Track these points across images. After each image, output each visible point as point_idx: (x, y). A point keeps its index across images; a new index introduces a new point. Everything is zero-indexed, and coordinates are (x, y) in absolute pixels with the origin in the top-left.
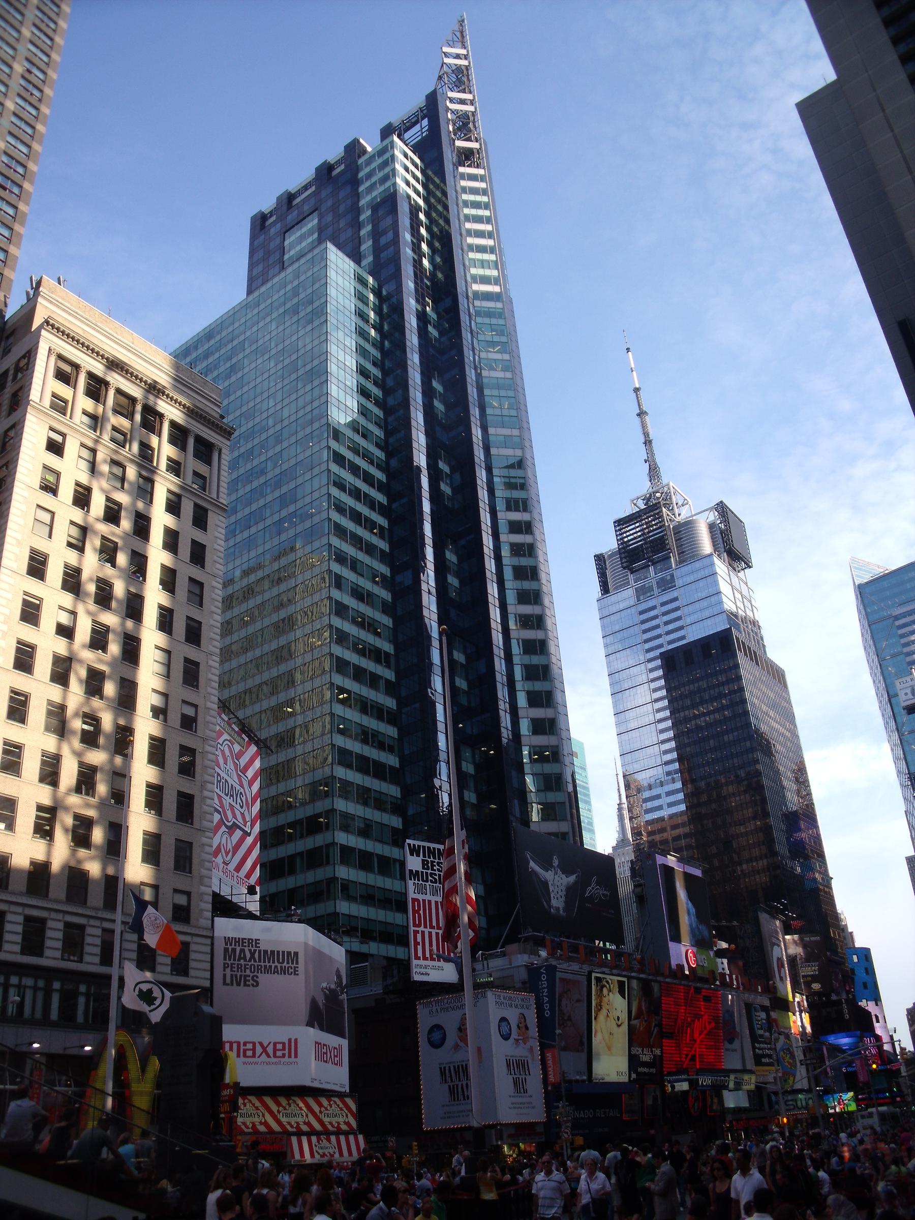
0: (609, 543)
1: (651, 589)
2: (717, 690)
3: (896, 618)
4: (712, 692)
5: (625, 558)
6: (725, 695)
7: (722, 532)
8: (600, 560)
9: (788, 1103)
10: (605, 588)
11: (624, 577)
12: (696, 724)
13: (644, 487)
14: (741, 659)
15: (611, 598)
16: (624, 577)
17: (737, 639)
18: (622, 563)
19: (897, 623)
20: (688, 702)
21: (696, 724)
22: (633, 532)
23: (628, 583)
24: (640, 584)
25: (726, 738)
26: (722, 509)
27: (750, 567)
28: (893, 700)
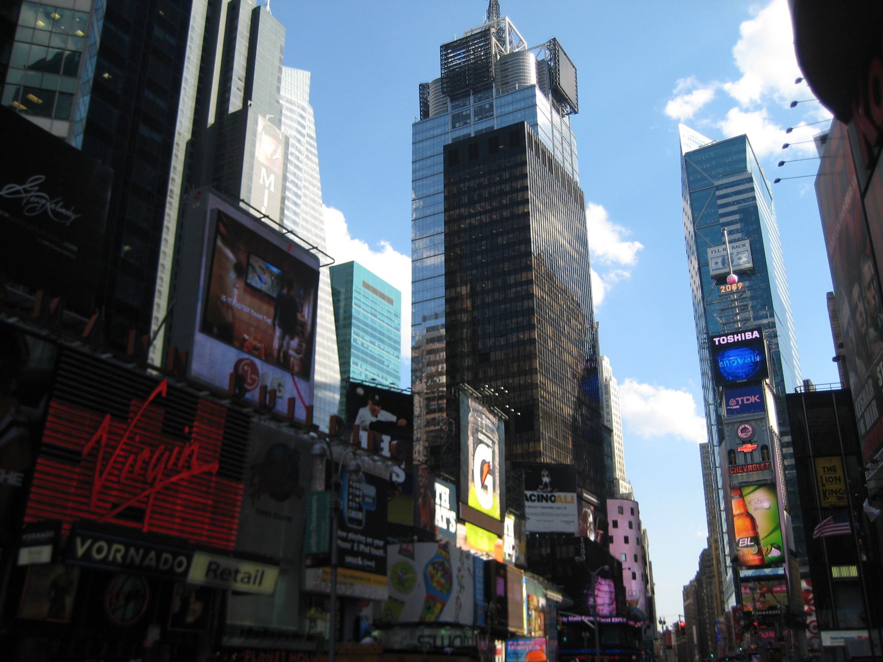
0: (433, 72)
1: (468, 116)
2: (498, 188)
3: (718, 188)
4: (493, 189)
5: (447, 83)
6: (506, 194)
7: (550, 69)
8: (423, 87)
9: (422, 640)
10: (425, 113)
11: (444, 104)
12: (470, 224)
13: (477, 21)
14: (530, 155)
15: (429, 124)
16: (444, 104)
17: (530, 137)
18: (442, 88)
19: (718, 193)
20: (465, 199)
21: (470, 224)
22: (457, 60)
23: (447, 111)
24: (457, 111)
25: (500, 239)
26: (554, 46)
27: (576, 113)
28: (703, 269)
